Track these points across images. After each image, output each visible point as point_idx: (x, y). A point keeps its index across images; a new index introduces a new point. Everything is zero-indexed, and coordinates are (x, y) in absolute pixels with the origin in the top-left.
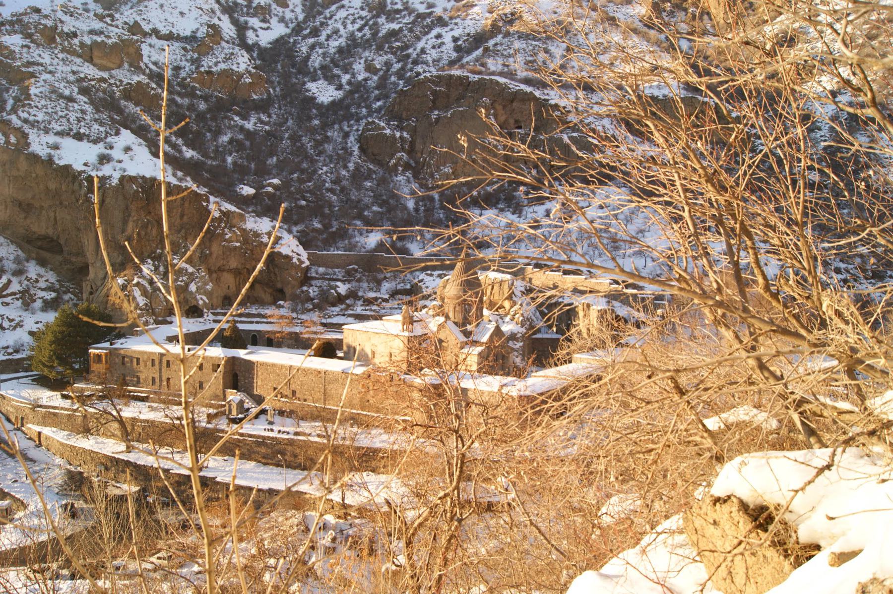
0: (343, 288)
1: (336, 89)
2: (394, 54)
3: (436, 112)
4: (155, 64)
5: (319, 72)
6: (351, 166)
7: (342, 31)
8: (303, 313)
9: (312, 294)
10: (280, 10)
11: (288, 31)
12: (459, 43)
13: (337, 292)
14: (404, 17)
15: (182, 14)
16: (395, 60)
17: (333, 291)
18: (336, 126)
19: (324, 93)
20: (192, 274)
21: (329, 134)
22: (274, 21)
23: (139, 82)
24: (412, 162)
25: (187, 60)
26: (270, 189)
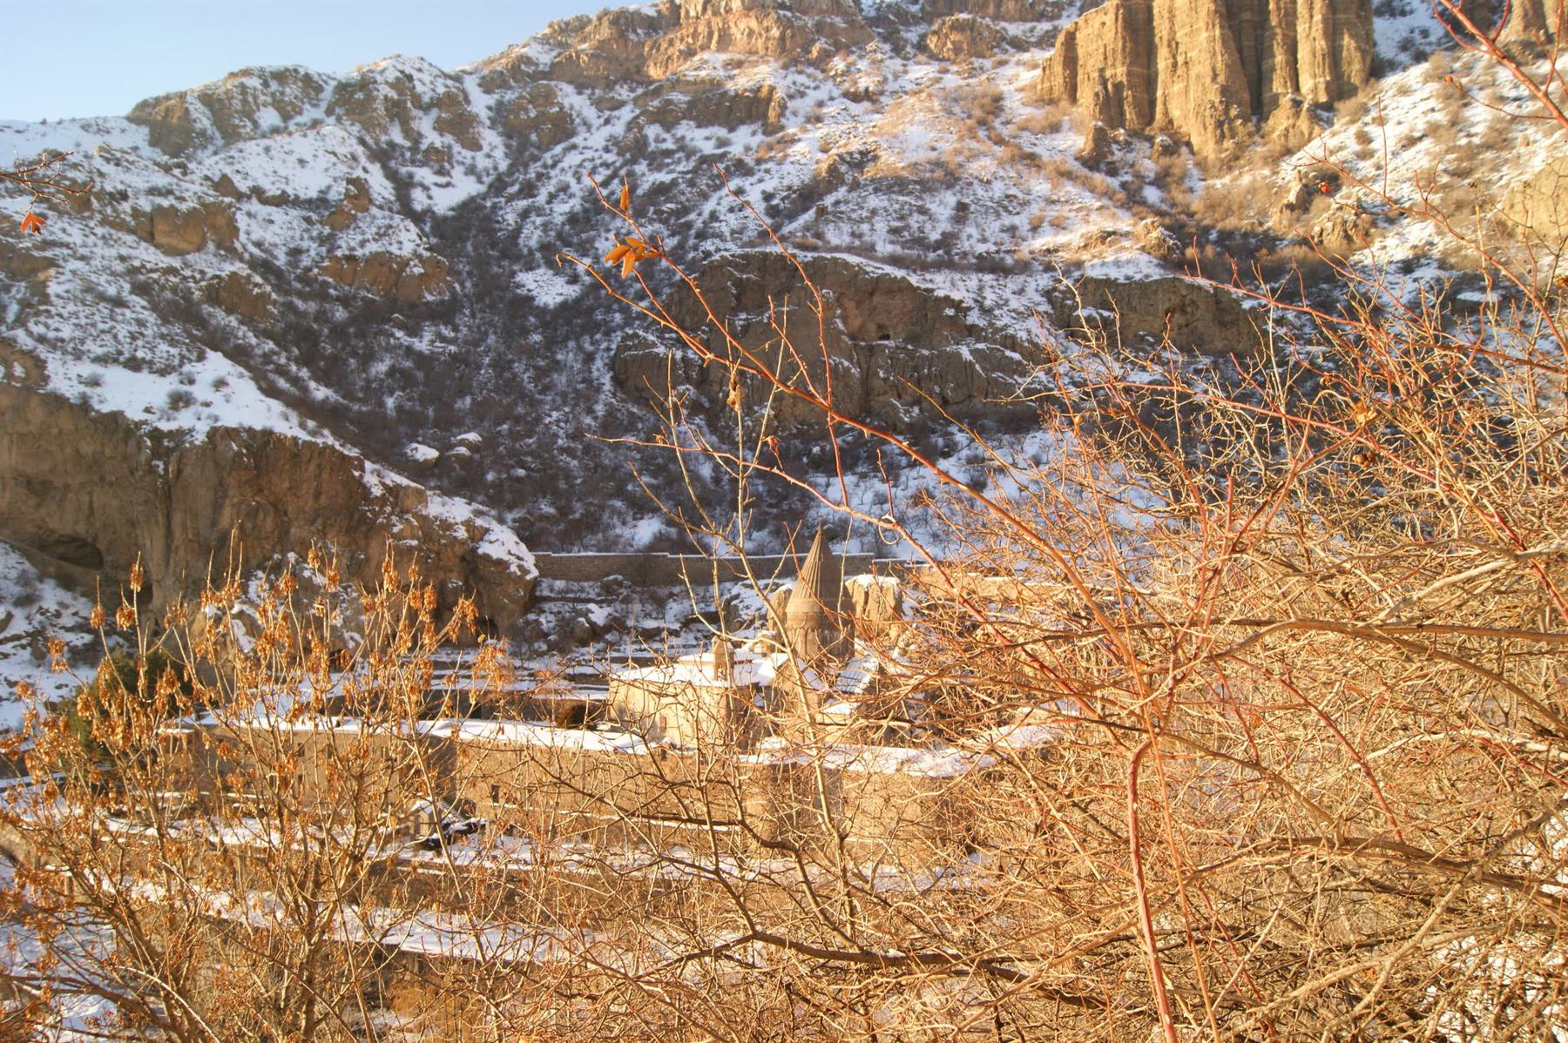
0: (599, 615)
1: (569, 283)
2: (665, 222)
3: (743, 316)
4: (258, 244)
5: (538, 255)
6: (600, 409)
7: (574, 187)
8: (529, 659)
9: (545, 626)
10: (468, 154)
11: (482, 189)
12: (775, 202)
13: (589, 621)
14: (679, 162)
15: (302, 162)
16: (666, 233)
17: (582, 619)
18: (571, 344)
19: (547, 289)
20: (335, 595)
21: (560, 357)
22: (457, 173)
23: (234, 274)
24: (703, 400)
25: (312, 238)
26: (463, 450)
